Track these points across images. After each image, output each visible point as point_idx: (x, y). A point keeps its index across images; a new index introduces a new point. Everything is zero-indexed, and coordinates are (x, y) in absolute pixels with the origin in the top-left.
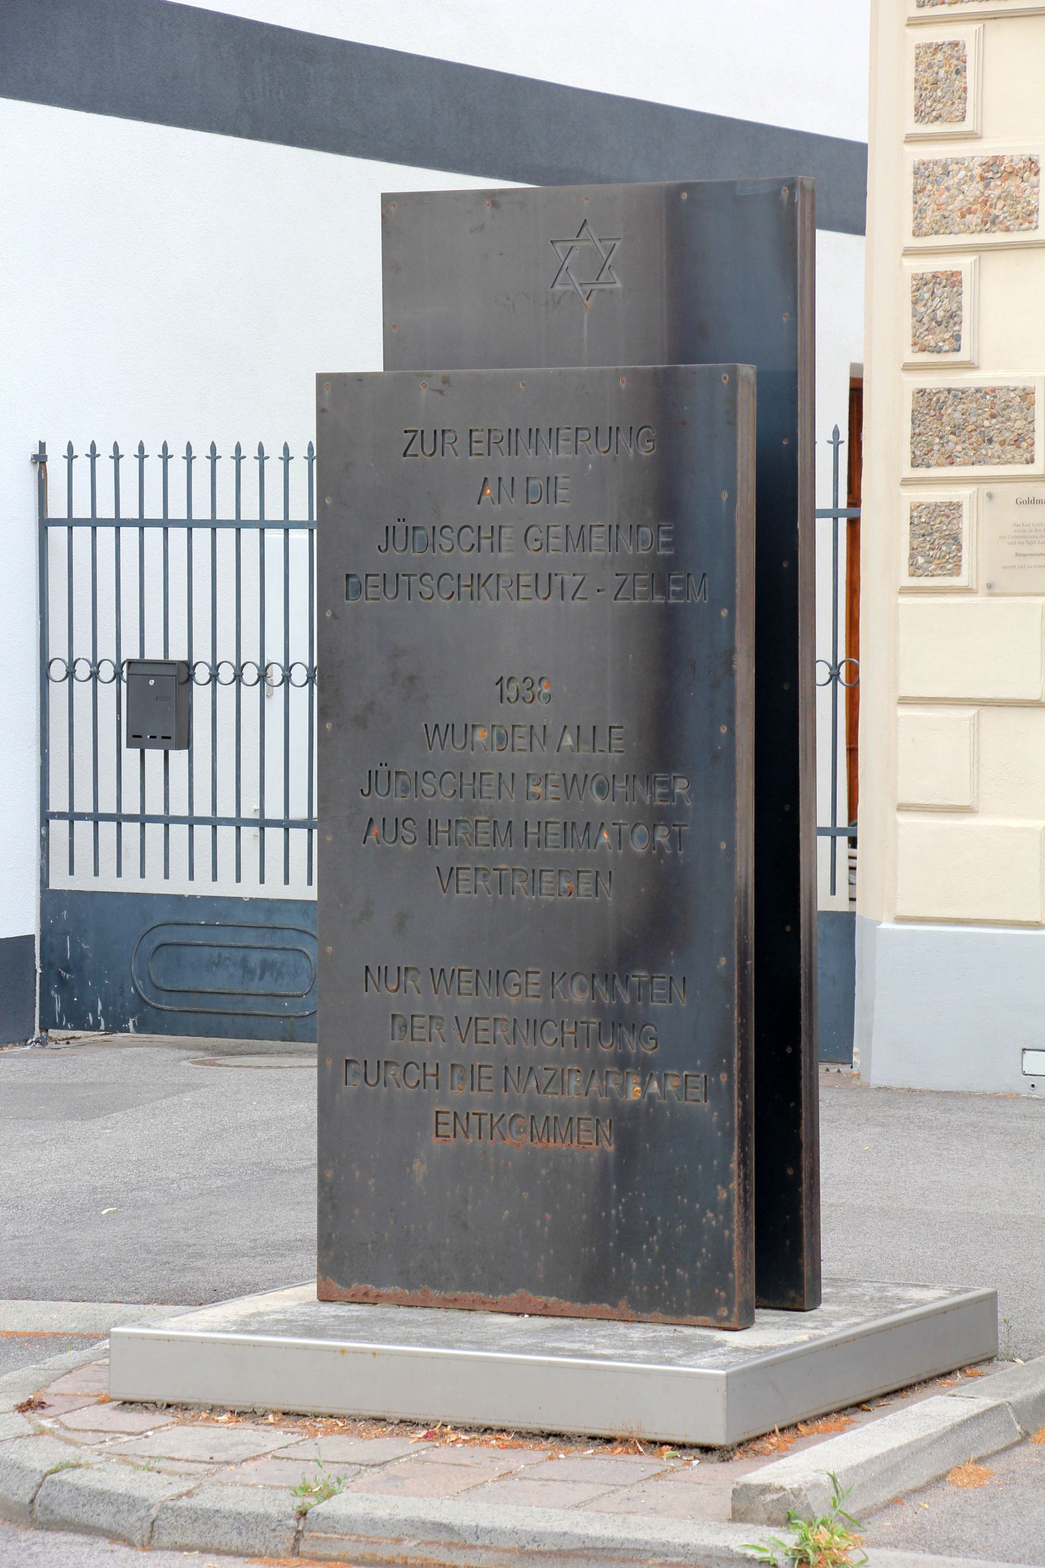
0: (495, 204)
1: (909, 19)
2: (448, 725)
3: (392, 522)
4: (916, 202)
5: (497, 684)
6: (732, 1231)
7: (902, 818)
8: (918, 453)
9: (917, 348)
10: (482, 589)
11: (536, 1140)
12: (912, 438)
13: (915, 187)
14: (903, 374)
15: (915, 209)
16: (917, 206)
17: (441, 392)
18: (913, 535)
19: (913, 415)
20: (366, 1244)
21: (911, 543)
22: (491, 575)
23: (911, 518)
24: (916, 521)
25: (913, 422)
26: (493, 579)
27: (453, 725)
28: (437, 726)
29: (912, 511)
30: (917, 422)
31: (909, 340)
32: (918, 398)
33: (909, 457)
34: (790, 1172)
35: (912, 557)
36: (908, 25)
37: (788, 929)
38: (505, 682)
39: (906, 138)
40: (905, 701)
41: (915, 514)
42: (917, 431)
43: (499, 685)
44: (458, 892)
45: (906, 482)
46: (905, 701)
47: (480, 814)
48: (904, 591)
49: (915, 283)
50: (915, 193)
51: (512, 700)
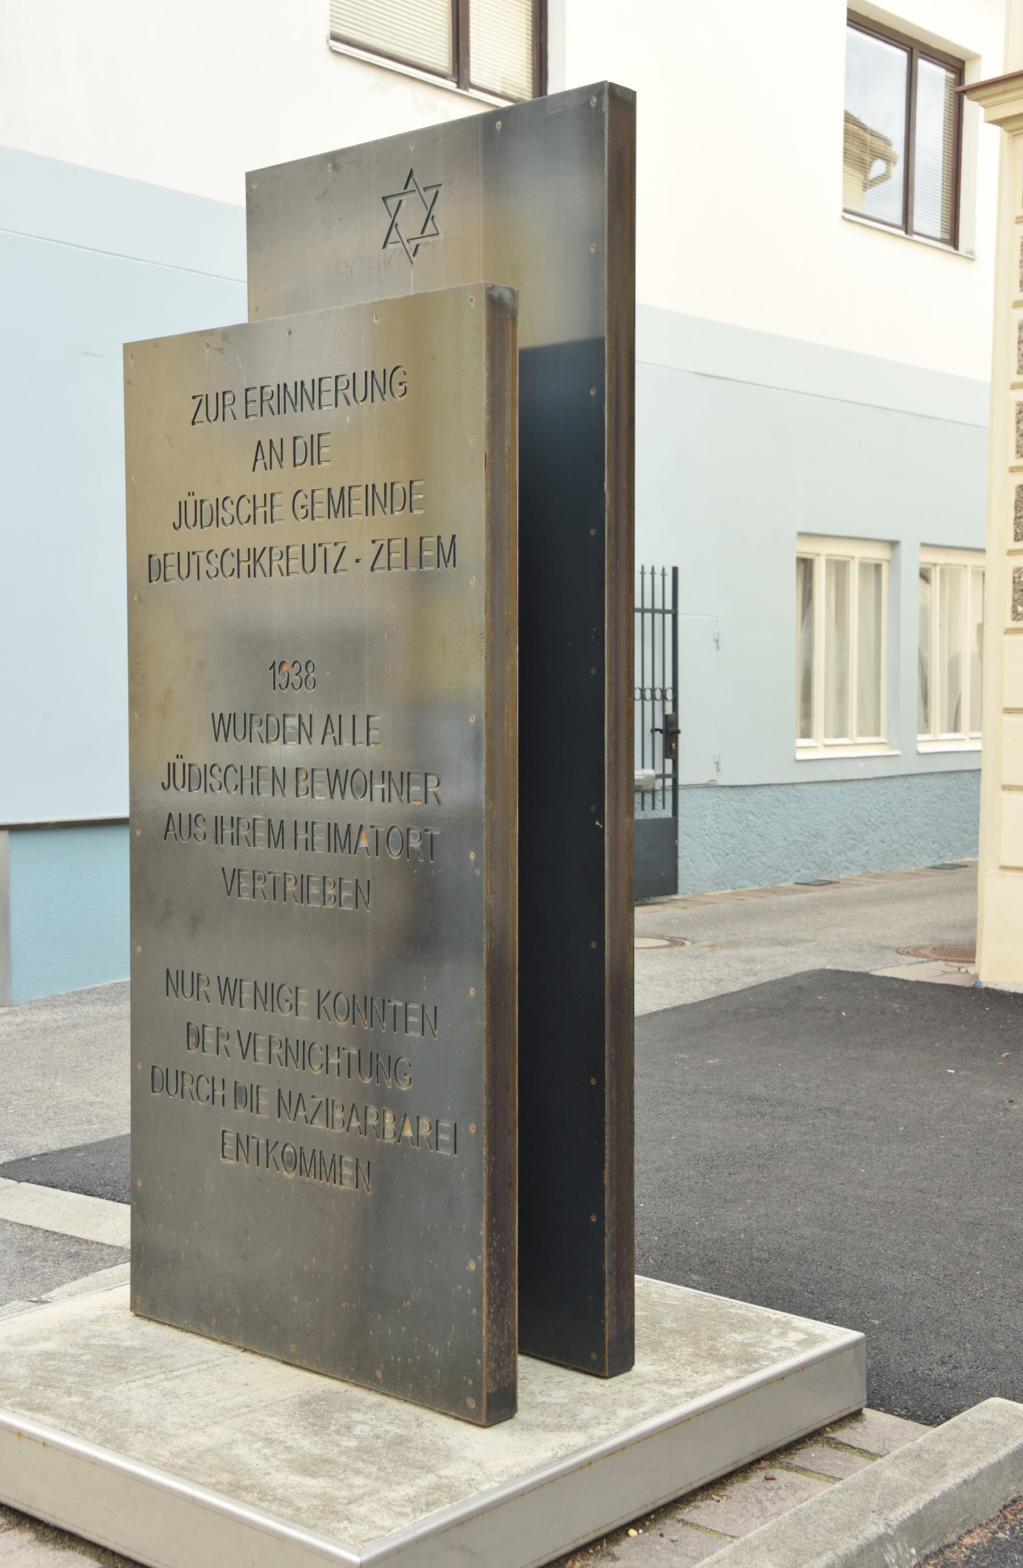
0: (336, 167)
1: (1018, 218)
2: (230, 714)
3: (184, 497)
4: (1020, 350)
5: (271, 669)
6: (480, 1309)
7: (1005, 795)
8: (1018, 531)
9: (1019, 455)
10: (258, 564)
11: (304, 1173)
12: (1015, 520)
13: (1019, 339)
14: (1010, 475)
15: (1019, 355)
16: (1021, 353)
17: (221, 350)
18: (1015, 591)
19: (1016, 504)
20: (168, 1262)
21: (1013, 597)
22: (265, 548)
23: (1014, 578)
24: (1017, 580)
25: (1016, 509)
26: (267, 551)
27: (235, 714)
28: (221, 715)
29: (1014, 573)
30: (1018, 509)
31: (1014, 449)
32: (1019, 491)
33: (1012, 534)
34: (593, 1219)
35: (1014, 607)
36: (1017, 223)
37: (593, 945)
38: (277, 666)
39: (1014, 304)
40: (1008, 711)
41: (1016, 575)
42: (1018, 515)
43: (272, 670)
44: (239, 896)
45: (1011, 553)
46: (1008, 711)
47: (258, 814)
48: (1008, 631)
49: (1018, 408)
50: (1019, 343)
51: (283, 686)
